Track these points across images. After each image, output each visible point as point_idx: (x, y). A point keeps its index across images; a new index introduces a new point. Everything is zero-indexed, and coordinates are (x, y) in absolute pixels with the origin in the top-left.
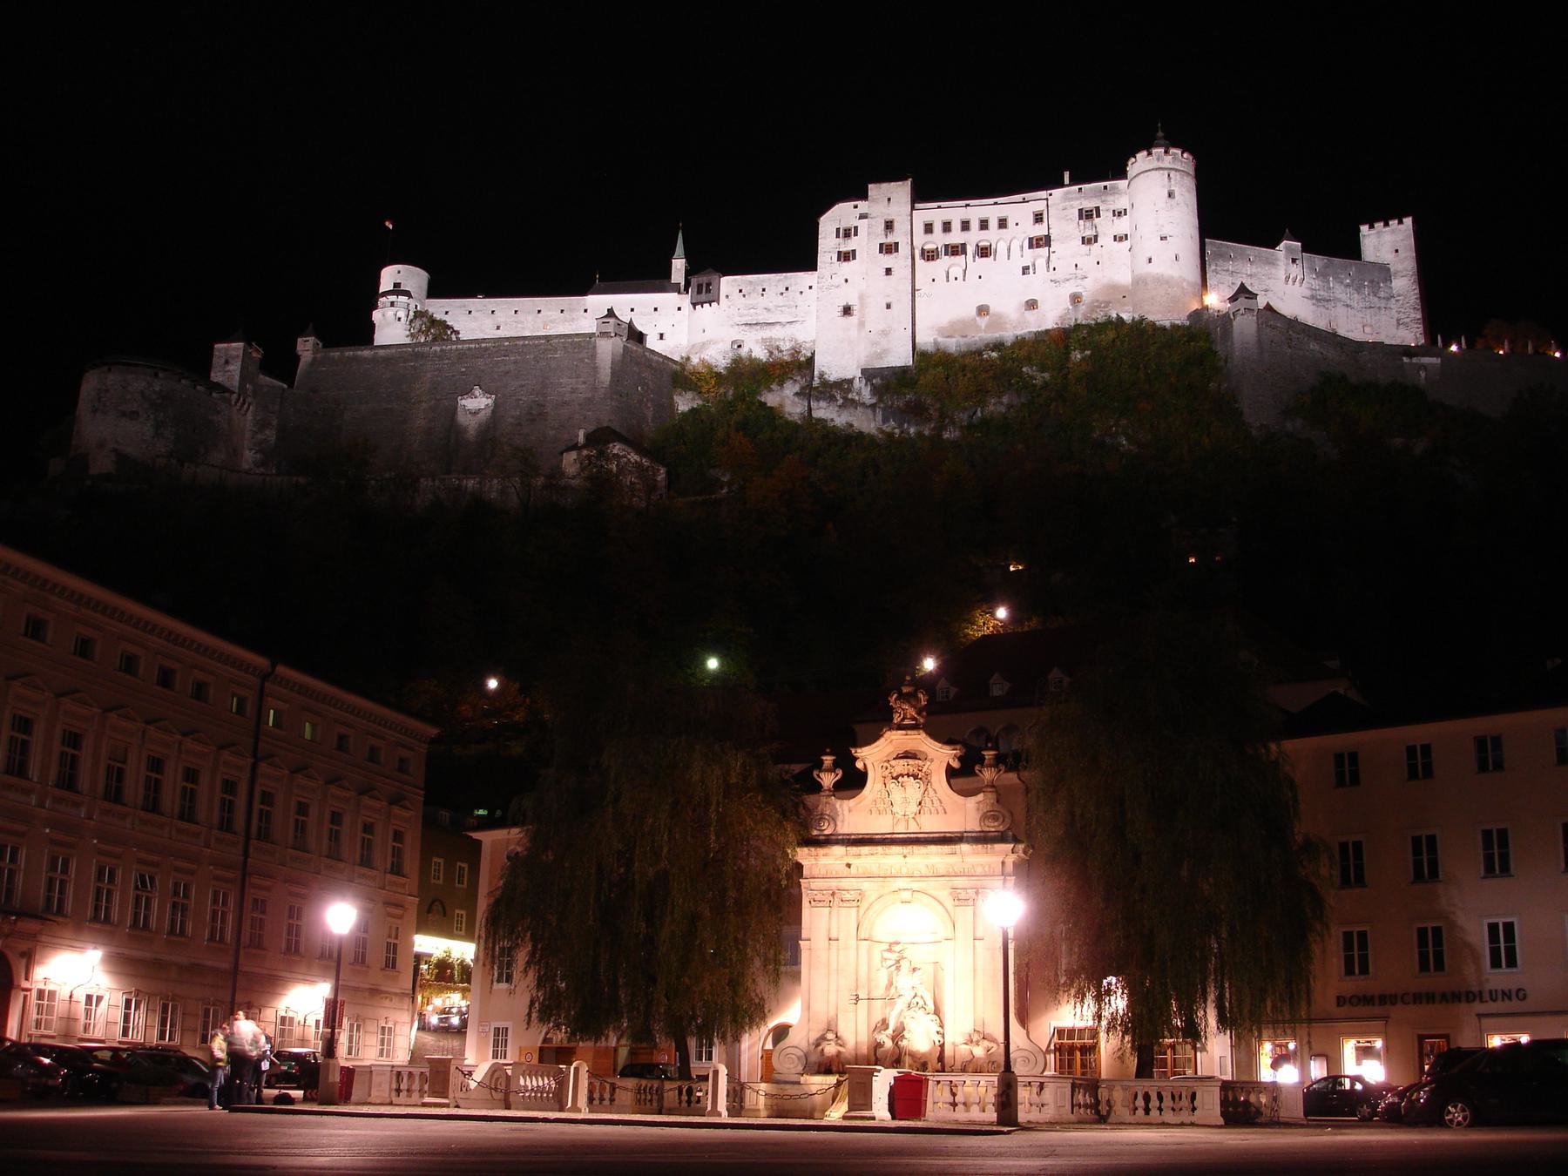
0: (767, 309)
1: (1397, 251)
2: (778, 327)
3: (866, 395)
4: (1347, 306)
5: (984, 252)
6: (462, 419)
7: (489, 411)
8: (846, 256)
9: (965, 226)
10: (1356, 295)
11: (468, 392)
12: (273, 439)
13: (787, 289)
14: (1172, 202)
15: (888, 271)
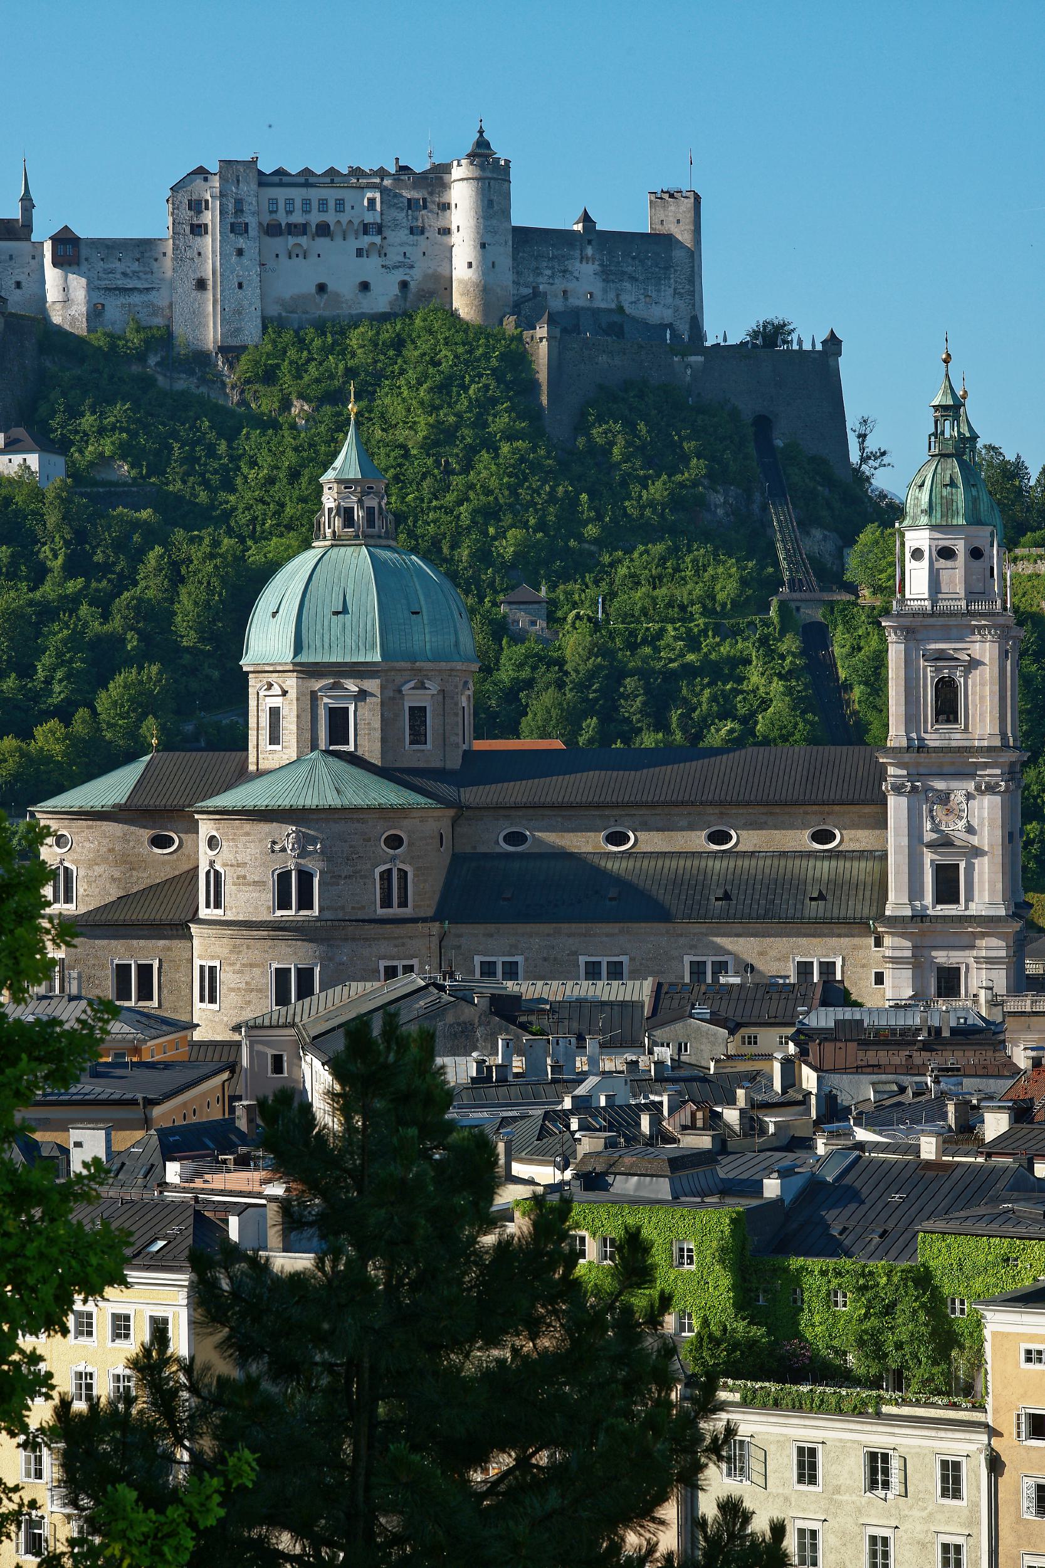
0: (124, 274)
1: (678, 222)
4: (633, 279)
5: (324, 230)
8: (198, 230)
9: (307, 203)
15: (240, 252)
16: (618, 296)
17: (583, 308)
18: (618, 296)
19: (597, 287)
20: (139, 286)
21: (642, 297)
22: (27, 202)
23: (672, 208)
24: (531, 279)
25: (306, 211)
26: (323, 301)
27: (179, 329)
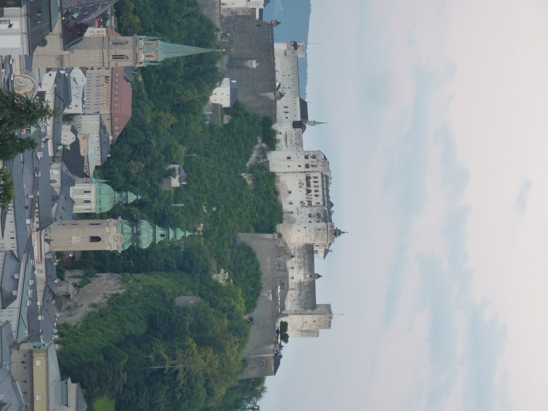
0: (291, 140)
1: (321, 311)
2: (285, 143)
3: (262, 161)
4: (300, 294)
5: (309, 191)
6: (249, 61)
7: (252, 67)
8: (306, 157)
9: (317, 186)
10: (304, 297)
11: (257, 62)
12: (240, 14)
13: (298, 145)
14: (317, 230)
15: (300, 166)
16: (293, 289)
17: (288, 275)
18: (293, 289)
19: (296, 280)
20: (288, 143)
21: (294, 298)
22: (315, 123)
23: (325, 309)
24: (297, 254)
25: (315, 186)
26: (286, 193)
27: (274, 152)
